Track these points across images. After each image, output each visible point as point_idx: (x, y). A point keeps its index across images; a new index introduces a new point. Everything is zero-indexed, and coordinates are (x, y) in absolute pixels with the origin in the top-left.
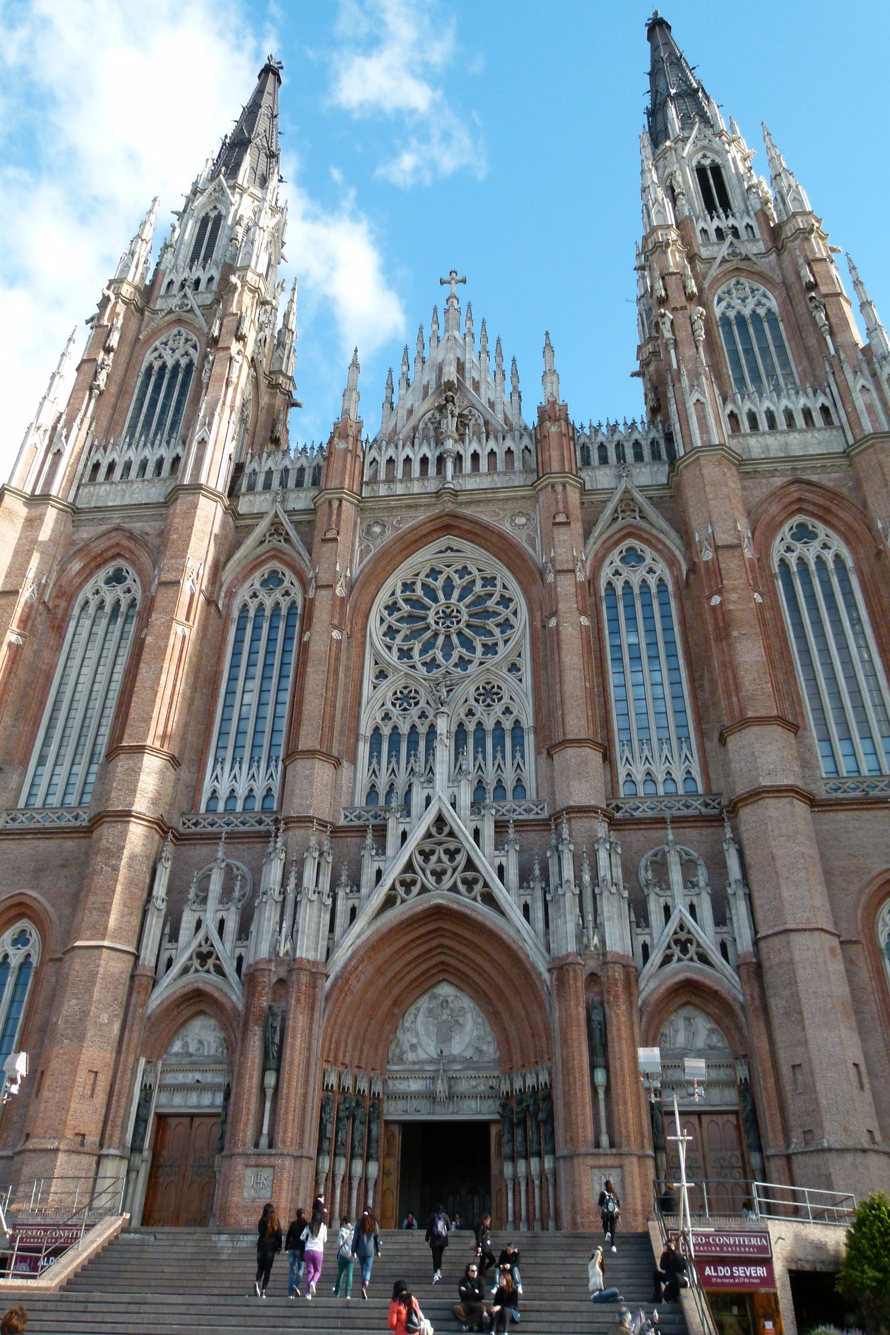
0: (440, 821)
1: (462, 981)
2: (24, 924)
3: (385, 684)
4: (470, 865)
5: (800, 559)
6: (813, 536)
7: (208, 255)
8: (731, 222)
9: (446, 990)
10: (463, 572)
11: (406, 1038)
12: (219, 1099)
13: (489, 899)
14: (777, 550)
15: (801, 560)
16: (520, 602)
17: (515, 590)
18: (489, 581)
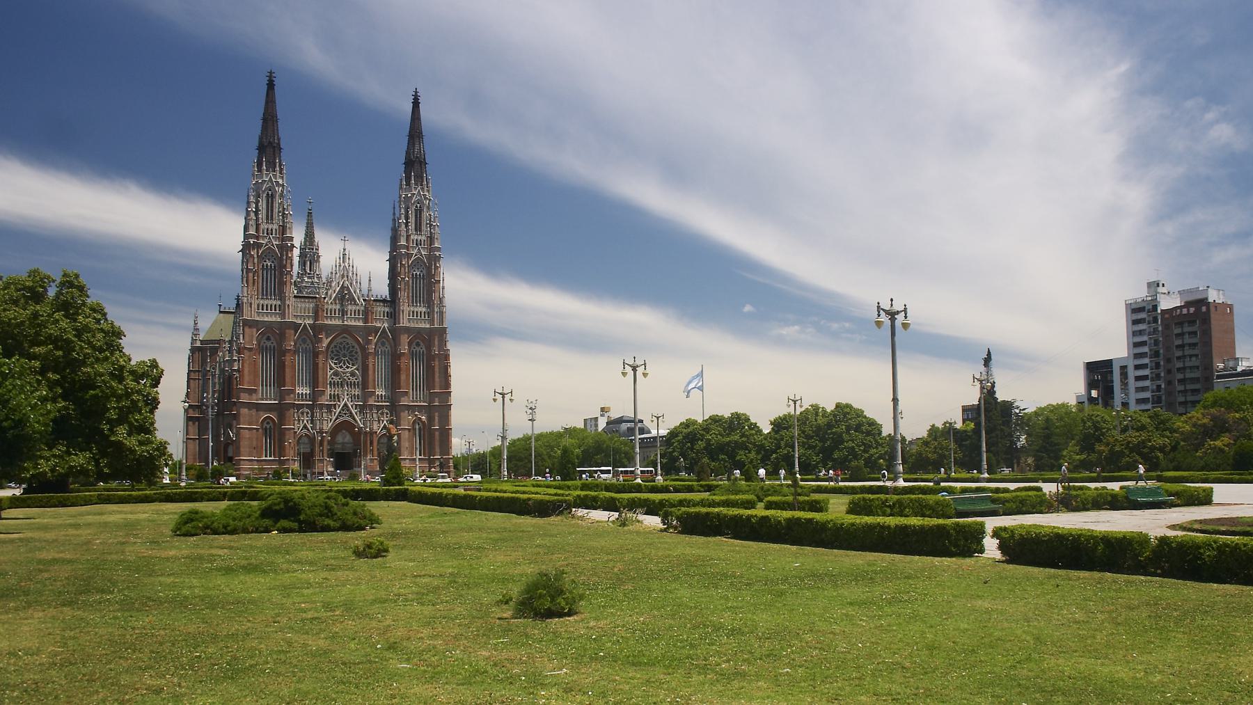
0: (346, 405)
1: (347, 430)
2: (268, 420)
3: (332, 371)
4: (351, 413)
5: (416, 351)
6: (419, 345)
7: (272, 219)
8: (419, 238)
9: (344, 431)
10: (348, 344)
11: (337, 439)
12: (309, 449)
13: (354, 419)
14: (412, 349)
15: (416, 351)
16: (360, 353)
17: (359, 350)
18: (353, 347)
